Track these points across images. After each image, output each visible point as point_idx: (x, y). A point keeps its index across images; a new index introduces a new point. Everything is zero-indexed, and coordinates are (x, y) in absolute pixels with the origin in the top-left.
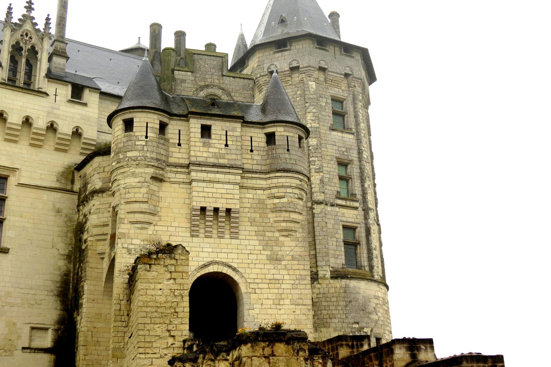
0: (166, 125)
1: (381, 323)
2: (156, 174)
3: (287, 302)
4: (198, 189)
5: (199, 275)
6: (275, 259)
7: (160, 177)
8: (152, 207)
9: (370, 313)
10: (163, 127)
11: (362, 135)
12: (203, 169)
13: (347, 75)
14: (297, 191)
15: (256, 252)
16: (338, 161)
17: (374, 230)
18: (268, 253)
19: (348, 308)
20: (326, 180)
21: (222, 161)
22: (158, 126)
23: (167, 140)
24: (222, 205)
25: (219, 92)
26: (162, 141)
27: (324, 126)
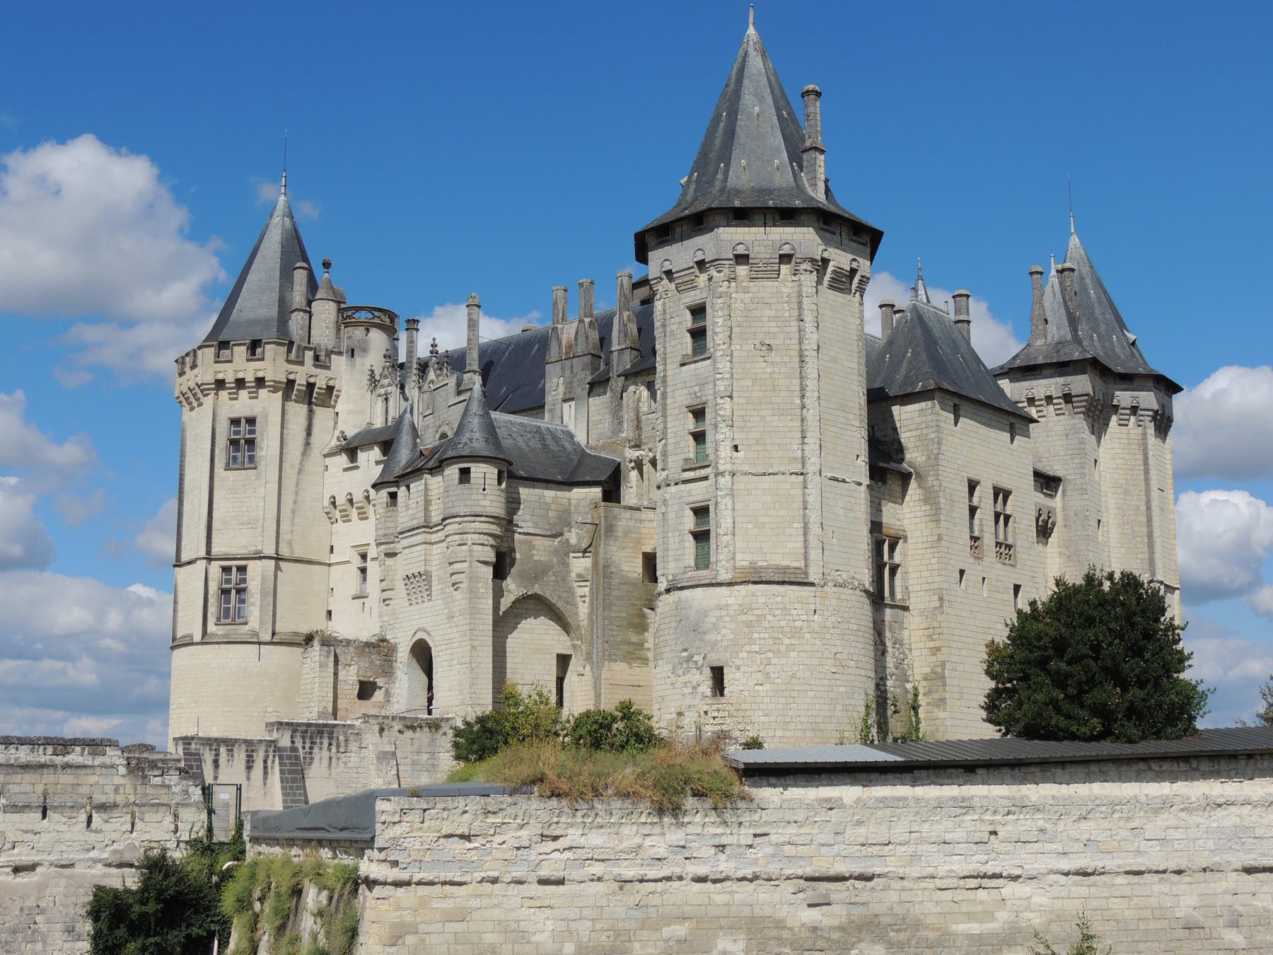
0: (396, 493)
1: (725, 643)
2: (386, 549)
3: (455, 662)
4: (405, 557)
5: (413, 642)
6: (450, 617)
7: (391, 551)
8: (389, 583)
9: (705, 633)
10: (393, 496)
11: (719, 354)
12: (405, 535)
13: (701, 265)
14: (457, 537)
15: (441, 612)
16: (690, 411)
17: (726, 505)
18: (446, 611)
19: (678, 630)
20: (670, 448)
21: (415, 523)
22: (385, 500)
23: (397, 511)
24: (415, 572)
25: (445, 429)
26: (389, 514)
27: (673, 363)
